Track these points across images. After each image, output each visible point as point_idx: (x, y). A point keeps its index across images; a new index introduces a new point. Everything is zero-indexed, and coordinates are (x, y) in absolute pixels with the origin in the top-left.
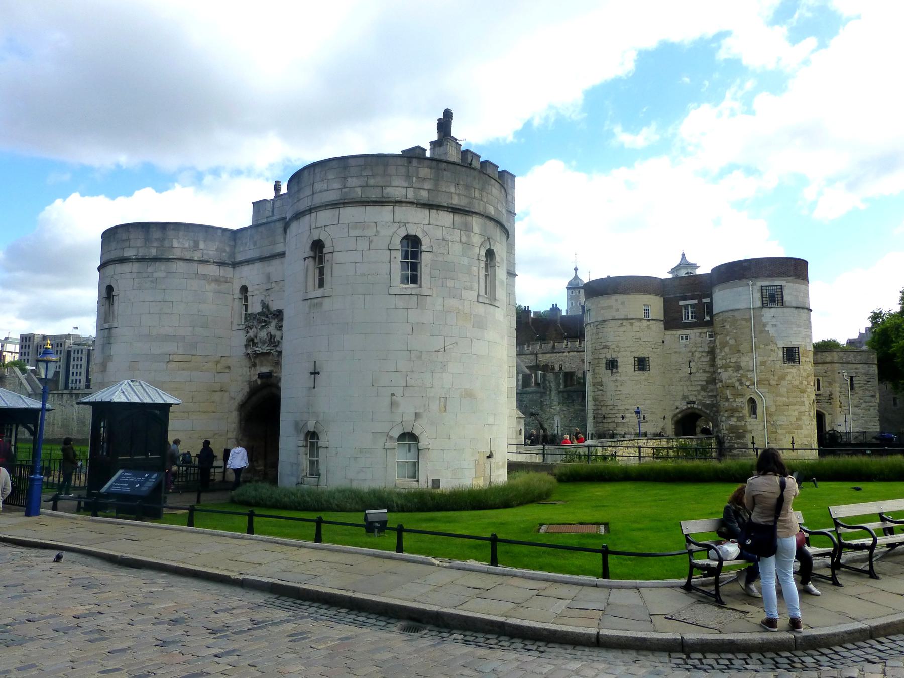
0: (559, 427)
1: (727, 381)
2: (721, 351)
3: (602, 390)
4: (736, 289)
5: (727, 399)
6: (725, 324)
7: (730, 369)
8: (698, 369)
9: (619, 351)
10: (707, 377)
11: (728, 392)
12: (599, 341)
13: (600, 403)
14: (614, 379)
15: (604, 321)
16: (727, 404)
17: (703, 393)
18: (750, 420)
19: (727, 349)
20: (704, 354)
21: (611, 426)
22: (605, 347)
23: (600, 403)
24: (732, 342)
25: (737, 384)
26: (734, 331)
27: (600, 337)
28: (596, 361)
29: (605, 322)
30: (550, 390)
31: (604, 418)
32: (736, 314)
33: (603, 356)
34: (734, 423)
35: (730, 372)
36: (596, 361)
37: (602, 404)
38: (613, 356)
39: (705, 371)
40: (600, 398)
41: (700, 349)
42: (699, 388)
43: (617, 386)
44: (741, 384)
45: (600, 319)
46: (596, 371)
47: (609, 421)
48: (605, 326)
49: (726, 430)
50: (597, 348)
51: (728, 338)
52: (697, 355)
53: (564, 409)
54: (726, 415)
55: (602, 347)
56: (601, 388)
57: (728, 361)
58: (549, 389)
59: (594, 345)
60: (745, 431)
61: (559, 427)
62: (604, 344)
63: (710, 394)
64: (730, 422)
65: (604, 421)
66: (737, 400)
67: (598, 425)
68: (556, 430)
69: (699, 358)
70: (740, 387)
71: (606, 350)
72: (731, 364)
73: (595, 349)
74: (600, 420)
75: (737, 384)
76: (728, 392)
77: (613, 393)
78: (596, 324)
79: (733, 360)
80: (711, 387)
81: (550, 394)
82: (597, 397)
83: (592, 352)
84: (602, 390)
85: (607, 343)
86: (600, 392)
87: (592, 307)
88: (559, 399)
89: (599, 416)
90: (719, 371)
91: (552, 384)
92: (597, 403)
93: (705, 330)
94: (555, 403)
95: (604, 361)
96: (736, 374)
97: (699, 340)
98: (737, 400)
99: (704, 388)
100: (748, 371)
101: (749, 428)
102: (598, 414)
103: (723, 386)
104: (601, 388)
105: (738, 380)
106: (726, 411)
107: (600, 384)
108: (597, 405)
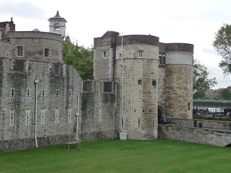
0: (101, 116)
1: (181, 94)
2: (178, 80)
3: (150, 96)
4: (187, 56)
5: (180, 102)
6: (181, 70)
7: (183, 89)
8: (161, 87)
9: (156, 76)
10: (163, 91)
11: (181, 99)
12: (150, 69)
13: (148, 103)
14: (155, 91)
15: (152, 60)
16: (180, 104)
17: (161, 98)
18: (188, 111)
19: (182, 81)
20: (163, 80)
21: (153, 116)
22: (153, 73)
23: (148, 103)
24: (184, 78)
25: (185, 96)
26: (186, 74)
27: (150, 67)
28: (147, 80)
29: (152, 60)
30: (98, 93)
31: (150, 111)
32: (187, 66)
33: (151, 78)
34: (183, 112)
35: (183, 90)
36: (147, 80)
37: (150, 103)
38: (155, 79)
39: (162, 88)
40: (149, 100)
41: (162, 78)
42: (160, 96)
43: (155, 94)
44: (187, 96)
45: (150, 58)
46: (147, 85)
47: (152, 112)
48: (152, 62)
49: (178, 115)
50: (148, 73)
51: (183, 76)
52: (161, 80)
53: (104, 105)
54: (179, 109)
55: (150, 73)
56: (149, 95)
57: (182, 86)
58: (97, 92)
59: (146, 71)
60: (187, 116)
61: (101, 116)
62: (152, 71)
63: (163, 99)
64: (181, 112)
65: (150, 113)
66: (185, 103)
67: (146, 115)
68: (99, 119)
69: (161, 82)
70: (186, 97)
71: (152, 75)
72: (183, 87)
73: (147, 73)
74: (148, 112)
75: (185, 96)
76: (181, 99)
77: (154, 98)
78: (147, 60)
79: (184, 86)
80: (164, 96)
81: (97, 95)
82: (147, 99)
83: (144, 75)
84: (150, 96)
85: (154, 72)
86: (149, 97)
87: (145, 50)
88: (102, 99)
89: (147, 110)
90: (175, 89)
91: (98, 89)
92: (147, 103)
93: (163, 70)
94: (99, 101)
95: (152, 81)
96: (185, 92)
97: (161, 74)
98: (185, 103)
99: (162, 97)
100: (189, 91)
101: (188, 114)
102: (147, 109)
103: (177, 96)
104: (149, 95)
105: (186, 94)
106: (179, 107)
107: (149, 92)
108: (147, 104)
